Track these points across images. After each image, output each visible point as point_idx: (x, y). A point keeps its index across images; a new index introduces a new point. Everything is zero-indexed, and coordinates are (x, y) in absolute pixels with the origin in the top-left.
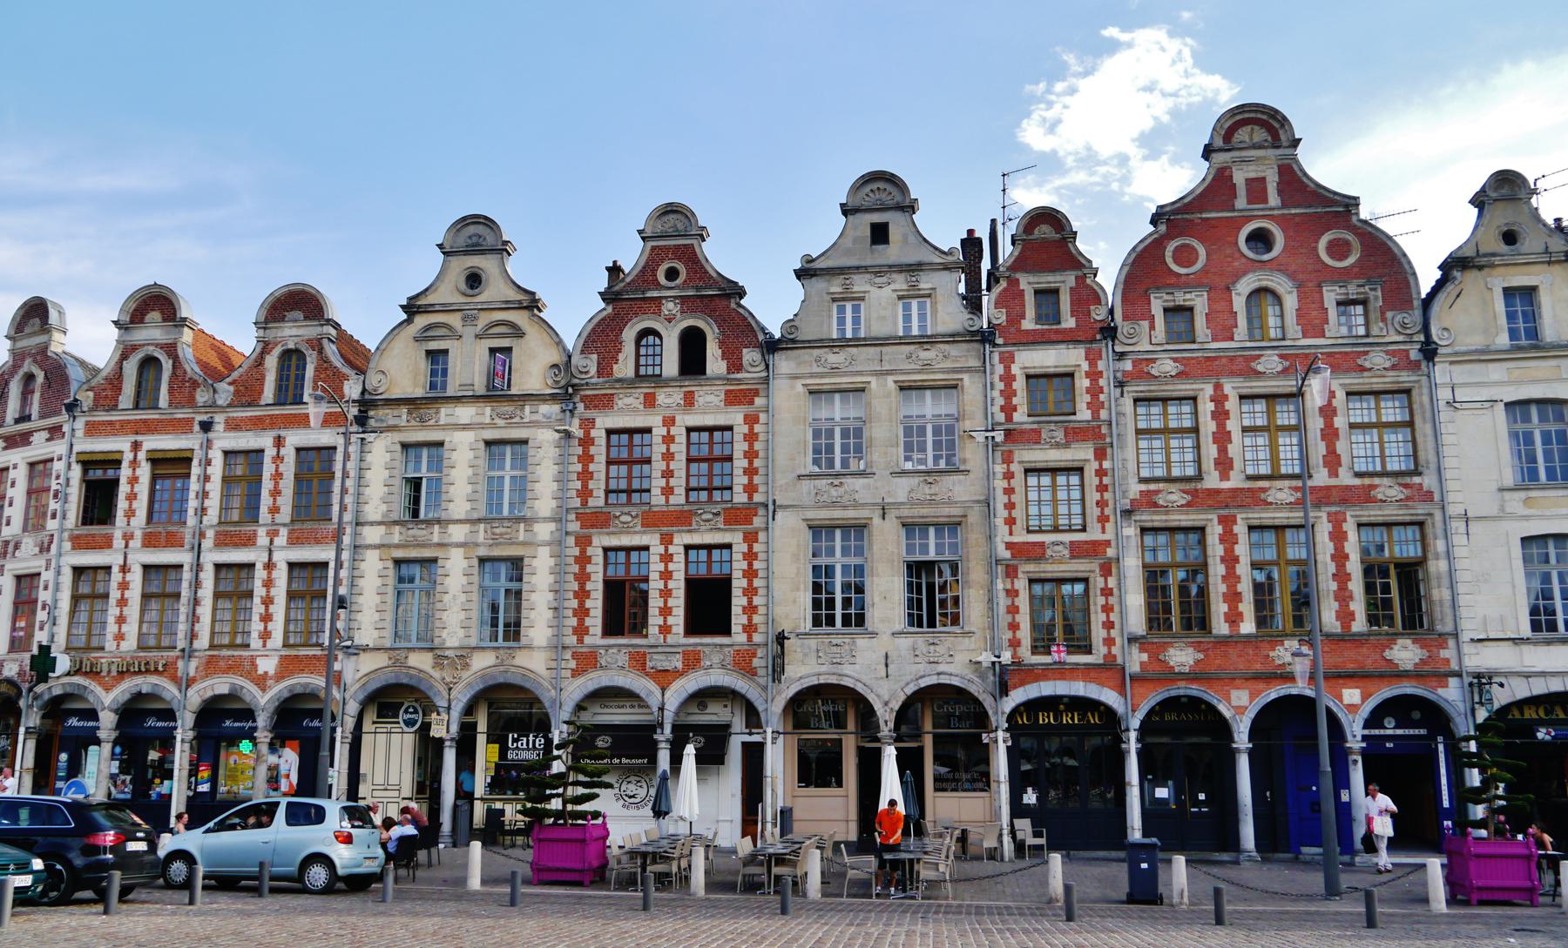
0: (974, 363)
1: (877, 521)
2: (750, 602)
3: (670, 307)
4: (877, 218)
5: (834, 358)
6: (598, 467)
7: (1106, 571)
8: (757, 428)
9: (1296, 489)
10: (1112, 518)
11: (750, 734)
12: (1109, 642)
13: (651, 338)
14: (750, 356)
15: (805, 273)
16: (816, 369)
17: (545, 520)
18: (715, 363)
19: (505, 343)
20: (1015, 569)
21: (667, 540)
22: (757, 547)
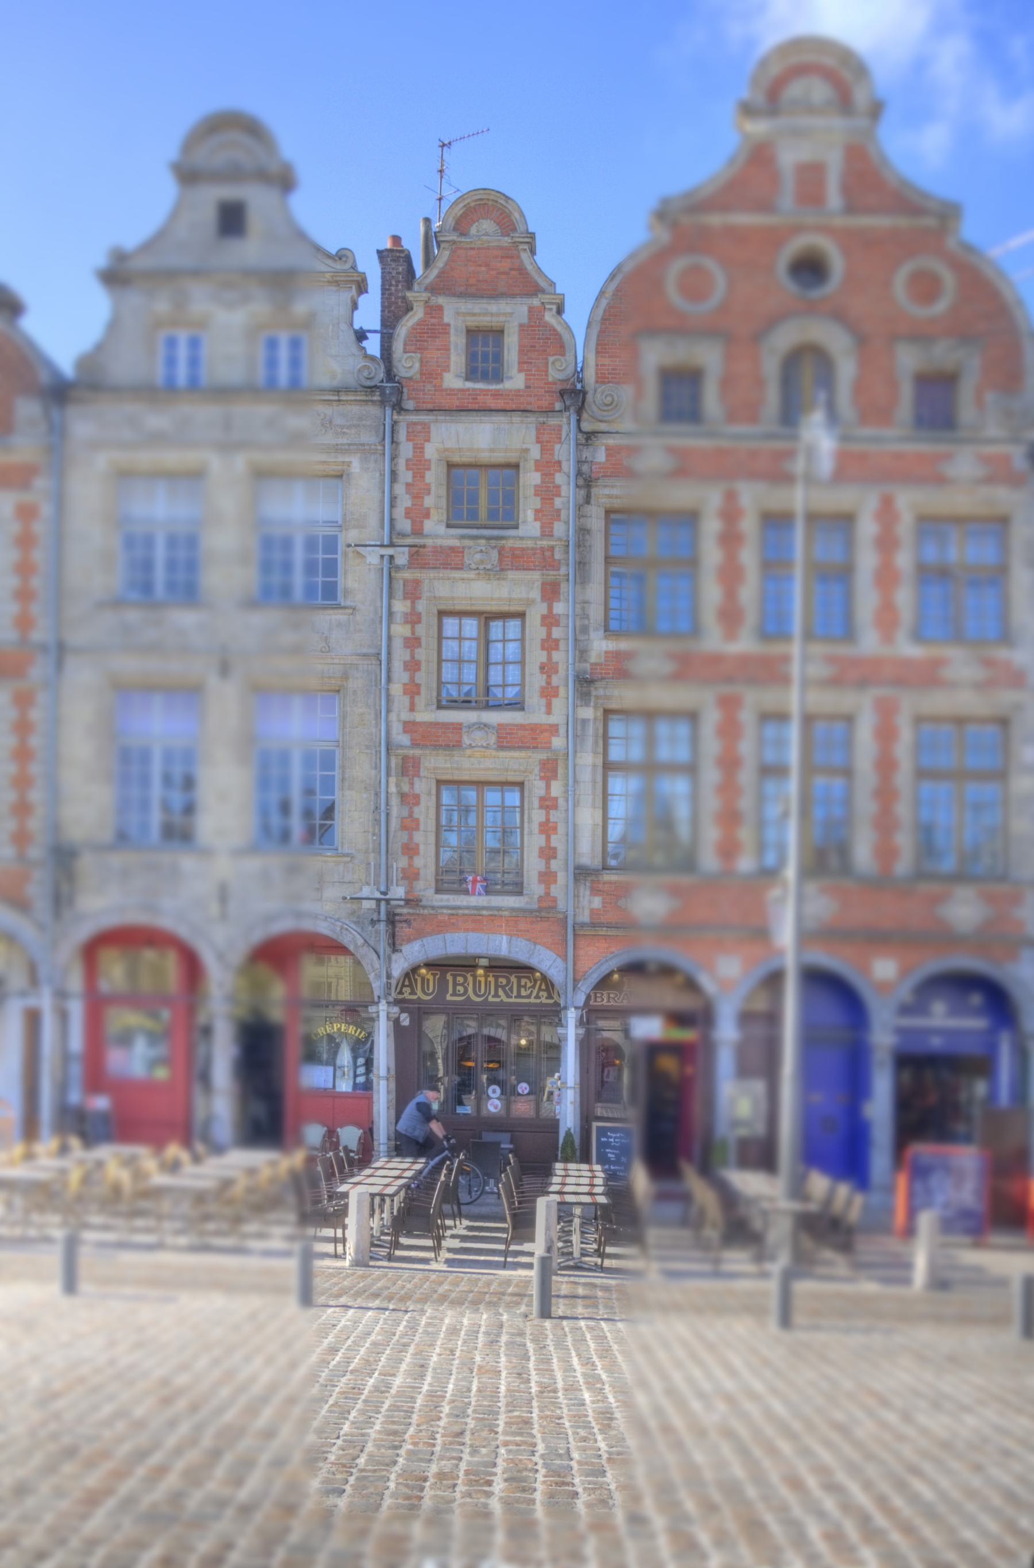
0: (369, 438)
1: (213, 681)
5: (157, 420)
7: (549, 770)
9: (831, 660)
10: (562, 691)
12: (547, 877)
14: (27, 409)
15: (116, 275)
20: (416, 763)
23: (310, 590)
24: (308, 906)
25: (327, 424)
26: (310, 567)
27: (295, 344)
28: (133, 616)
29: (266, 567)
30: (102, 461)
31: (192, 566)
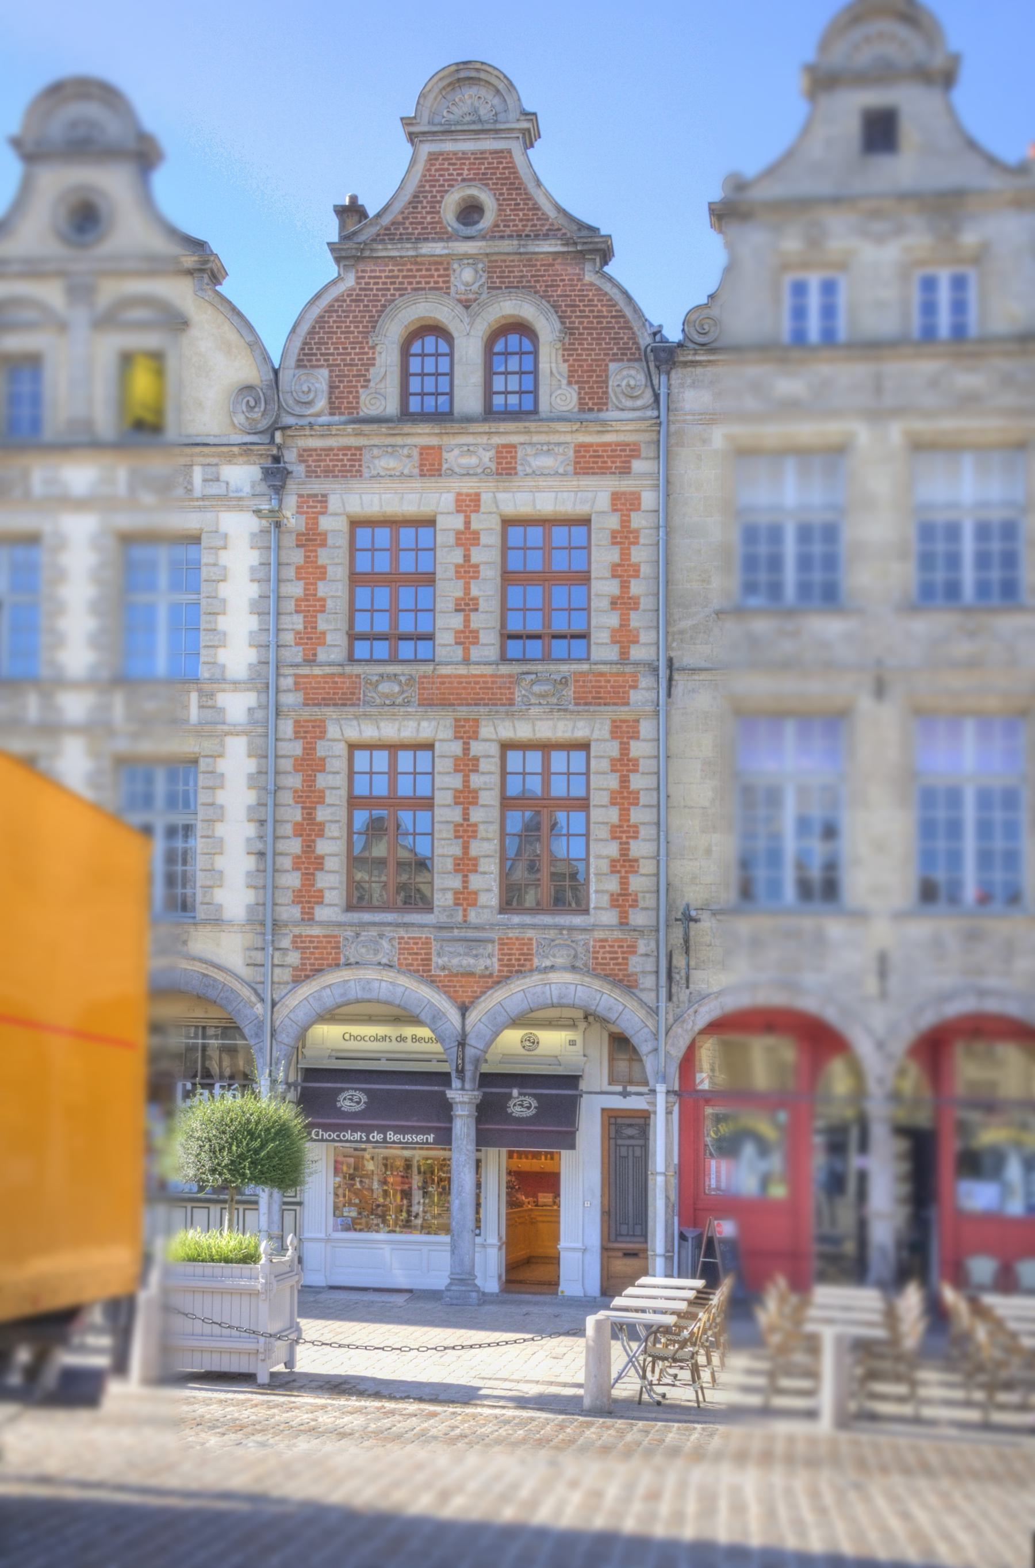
1: (865, 703)
2: (624, 851)
3: (465, 276)
4: (874, 98)
5: (789, 385)
6: (334, 589)
8: (638, 521)
11: (625, 1094)
13: (430, 341)
14: (625, 377)
15: (727, 213)
16: (750, 403)
17: (236, 685)
18: (558, 394)
19: (151, 340)
21: (466, 732)
22: (638, 749)
23: (983, 589)
24: (992, 981)
25: (1007, 381)
26: (983, 560)
27: (959, 283)
28: (761, 626)
29: (926, 561)
30: (718, 437)
31: (830, 562)
